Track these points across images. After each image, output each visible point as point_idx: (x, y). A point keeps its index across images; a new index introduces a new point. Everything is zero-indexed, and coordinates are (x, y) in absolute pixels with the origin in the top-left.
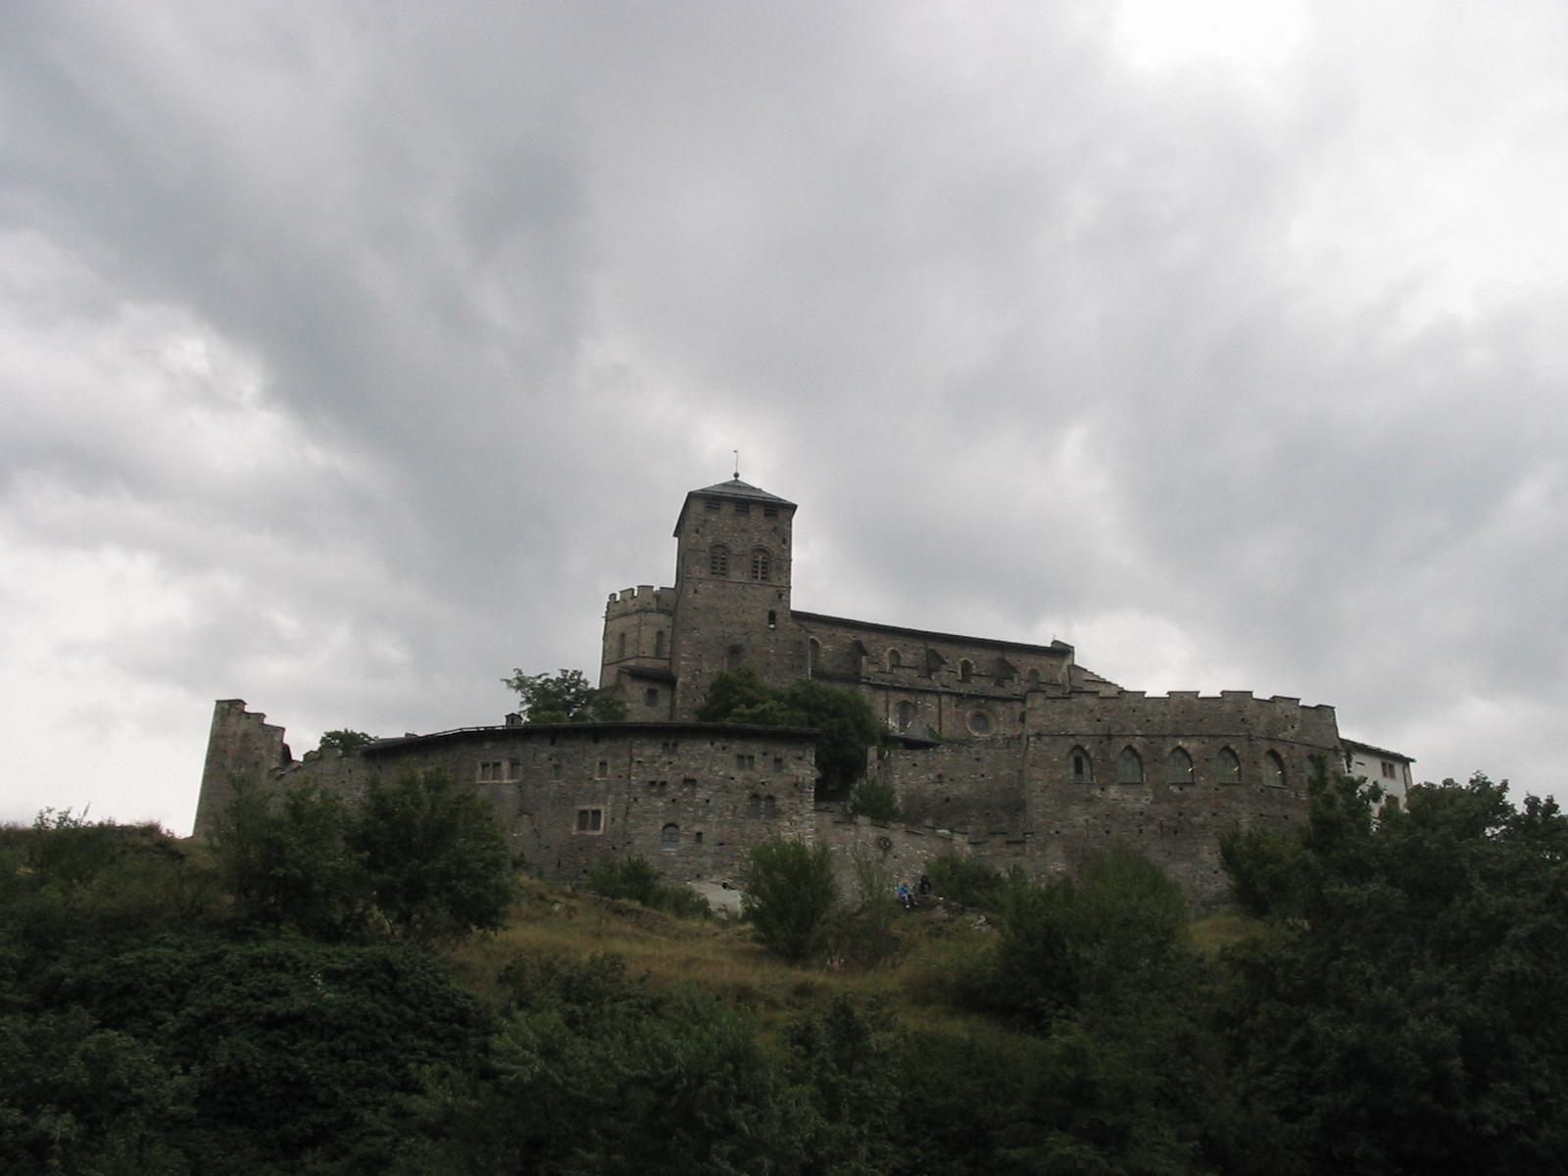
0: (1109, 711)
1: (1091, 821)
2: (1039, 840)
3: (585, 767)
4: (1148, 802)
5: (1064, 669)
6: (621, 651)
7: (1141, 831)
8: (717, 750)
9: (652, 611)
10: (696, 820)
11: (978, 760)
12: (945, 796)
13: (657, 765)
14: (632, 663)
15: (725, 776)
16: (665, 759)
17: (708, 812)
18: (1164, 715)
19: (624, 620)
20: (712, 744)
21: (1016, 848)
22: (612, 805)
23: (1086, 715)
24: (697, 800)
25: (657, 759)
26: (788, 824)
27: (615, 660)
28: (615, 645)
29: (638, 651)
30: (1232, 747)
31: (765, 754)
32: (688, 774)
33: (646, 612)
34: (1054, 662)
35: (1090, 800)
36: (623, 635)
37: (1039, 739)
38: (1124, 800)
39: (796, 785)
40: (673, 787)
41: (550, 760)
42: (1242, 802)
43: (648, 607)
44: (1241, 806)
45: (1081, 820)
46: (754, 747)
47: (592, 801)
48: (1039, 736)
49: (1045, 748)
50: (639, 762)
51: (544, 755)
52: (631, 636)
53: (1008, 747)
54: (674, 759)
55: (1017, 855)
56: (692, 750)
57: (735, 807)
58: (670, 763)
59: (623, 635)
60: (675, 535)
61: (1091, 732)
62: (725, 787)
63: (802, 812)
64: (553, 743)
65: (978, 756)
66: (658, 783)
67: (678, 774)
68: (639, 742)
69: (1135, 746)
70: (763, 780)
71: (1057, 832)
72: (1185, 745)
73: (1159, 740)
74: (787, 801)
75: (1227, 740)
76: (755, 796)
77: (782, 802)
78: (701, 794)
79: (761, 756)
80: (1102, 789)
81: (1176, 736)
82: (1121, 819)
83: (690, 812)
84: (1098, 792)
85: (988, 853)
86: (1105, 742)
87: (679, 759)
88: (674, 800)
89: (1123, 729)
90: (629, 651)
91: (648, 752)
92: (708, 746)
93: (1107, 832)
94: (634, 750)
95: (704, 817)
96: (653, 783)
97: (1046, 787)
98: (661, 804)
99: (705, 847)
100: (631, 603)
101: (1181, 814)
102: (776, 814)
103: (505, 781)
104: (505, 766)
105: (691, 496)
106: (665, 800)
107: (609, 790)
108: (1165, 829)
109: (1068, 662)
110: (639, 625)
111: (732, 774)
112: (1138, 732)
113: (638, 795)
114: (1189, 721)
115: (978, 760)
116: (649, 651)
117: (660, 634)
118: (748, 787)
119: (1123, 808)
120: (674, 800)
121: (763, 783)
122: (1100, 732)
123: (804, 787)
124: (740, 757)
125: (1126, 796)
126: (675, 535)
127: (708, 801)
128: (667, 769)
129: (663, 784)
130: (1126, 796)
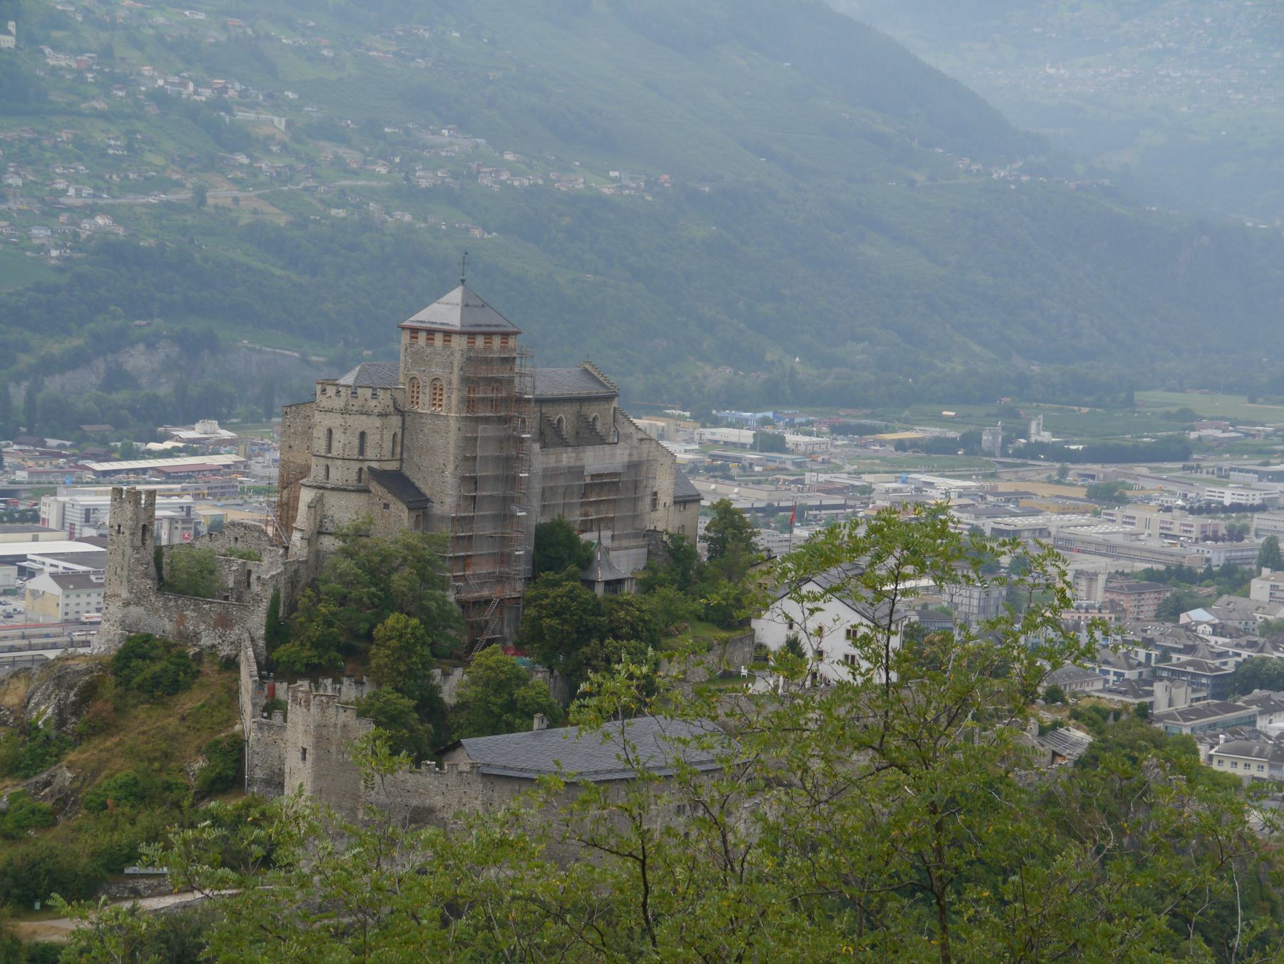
5: (612, 410)
6: (362, 450)
14: (375, 465)
19: (364, 418)
27: (356, 457)
28: (356, 442)
33: (386, 415)
34: (606, 406)
36: (363, 435)
52: (372, 439)
59: (363, 435)
90: (370, 453)
96: (679, 806)
100: (374, 403)
107: (657, 816)
109: (615, 404)
116: (388, 456)
117: (395, 435)
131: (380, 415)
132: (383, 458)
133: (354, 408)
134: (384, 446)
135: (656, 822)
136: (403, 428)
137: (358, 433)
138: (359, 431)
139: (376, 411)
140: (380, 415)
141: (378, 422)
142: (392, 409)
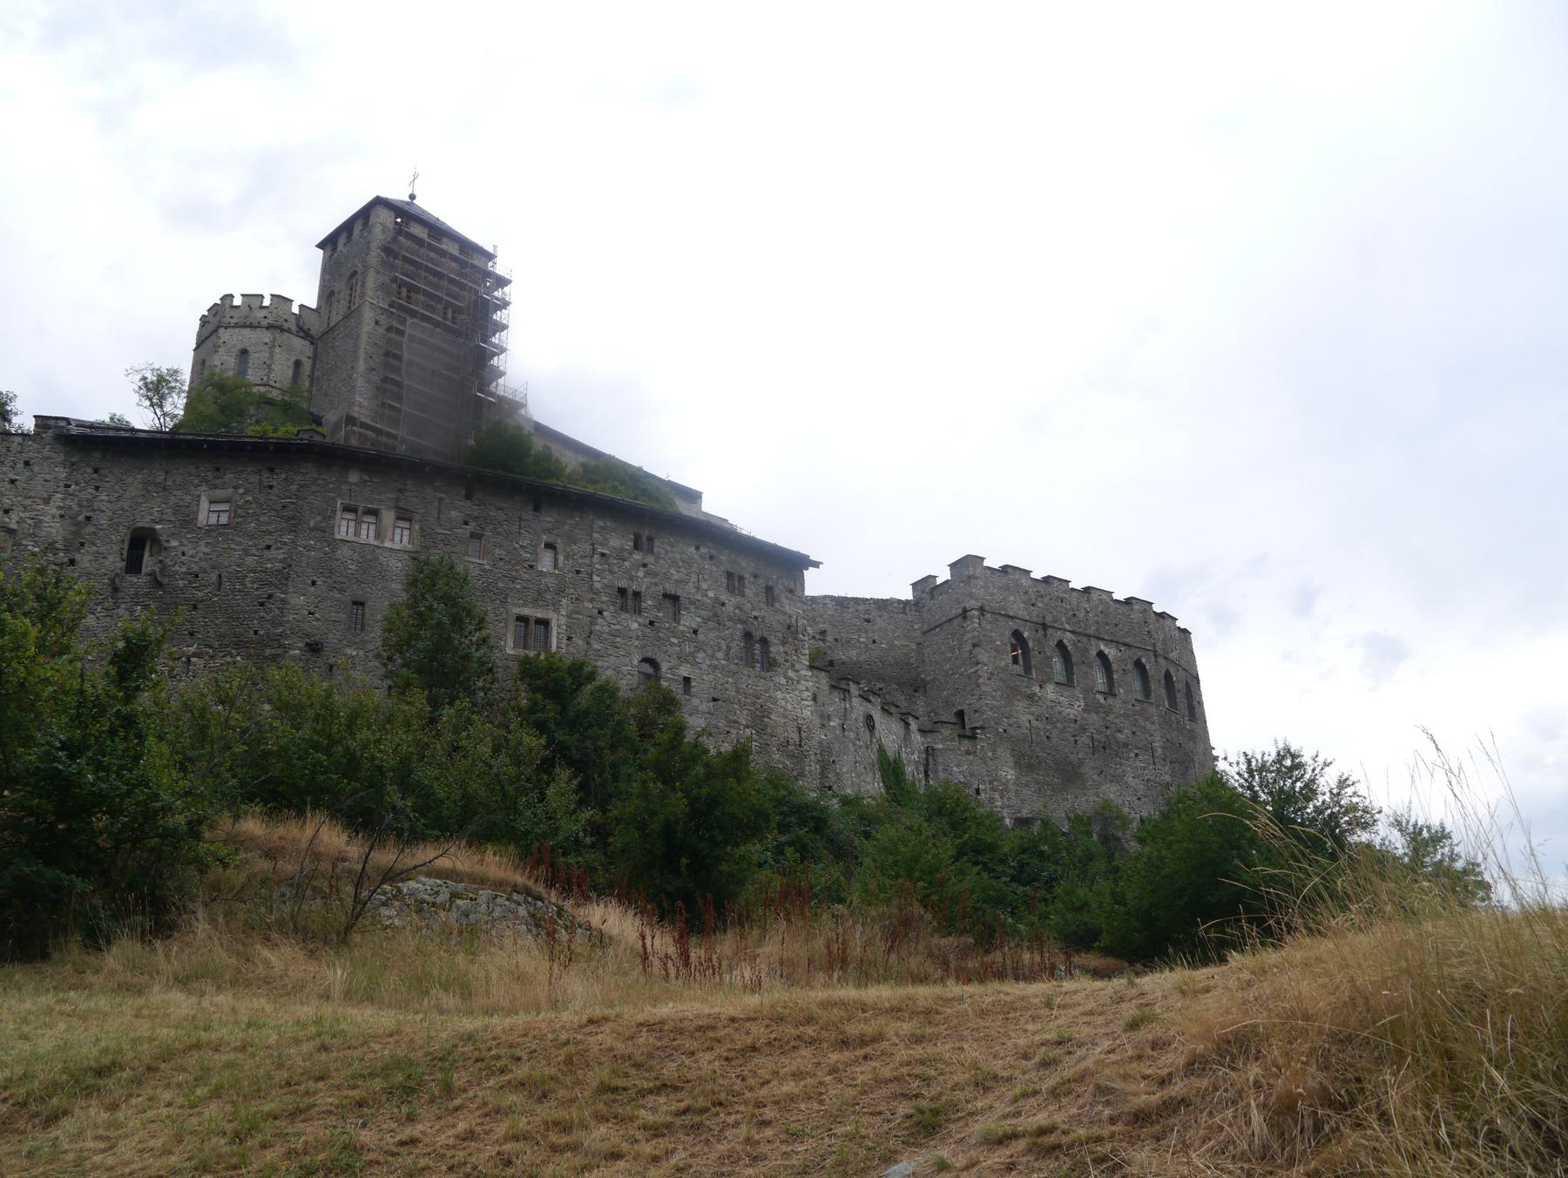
0: (1042, 597)
1: (1035, 723)
2: (989, 738)
3: (522, 547)
4: (1080, 709)
7: (1076, 741)
8: (702, 557)
9: (289, 331)
10: (682, 658)
11: (868, 621)
12: (829, 658)
13: (627, 564)
15: (716, 599)
16: (637, 556)
17: (698, 648)
18: (1087, 612)
19: (246, 332)
20: (697, 548)
21: (966, 744)
22: (568, 617)
23: (1022, 597)
24: (681, 628)
25: (626, 554)
26: (783, 681)
29: (269, 378)
30: (1144, 661)
31: (755, 576)
32: (670, 588)
33: (282, 330)
35: (1031, 697)
37: (983, 615)
38: (1059, 703)
39: (789, 627)
40: (650, 602)
41: (466, 523)
42: (1153, 723)
43: (286, 326)
44: (1154, 728)
45: (1025, 718)
46: (744, 564)
47: (538, 598)
48: (982, 610)
49: (988, 627)
50: (603, 555)
51: (454, 514)
52: (255, 358)
53: (904, 613)
54: (650, 559)
55: (968, 753)
56: (672, 552)
57: (729, 648)
58: (645, 565)
59: (244, 352)
60: (321, 245)
61: (1027, 618)
62: (715, 615)
63: (798, 666)
64: (468, 497)
65: (867, 616)
66: (630, 592)
67: (656, 584)
68: (601, 523)
69: (1065, 641)
70: (755, 613)
71: (1005, 731)
72: (1106, 651)
73: (1085, 640)
74: (781, 649)
75: (1140, 654)
76: (748, 636)
77: (776, 650)
78: (688, 620)
79: (752, 579)
80: (1041, 687)
81: (1099, 639)
82: (1059, 725)
83: (672, 644)
84: (1037, 689)
85: (940, 746)
86: (1041, 632)
87: (657, 560)
88: (651, 623)
89: (1055, 622)
91: (615, 542)
92: (692, 550)
93: (1048, 738)
94: (596, 535)
95: (692, 654)
96: (622, 591)
97: (992, 674)
98: (635, 626)
99: (695, 702)
101: (1107, 728)
102: (770, 664)
103: (388, 544)
104: (388, 517)
105: (378, 202)
106: (641, 620)
107: (560, 591)
108: (1096, 744)
110: (272, 346)
111: (723, 598)
112: (1067, 627)
113: (604, 606)
114: (1107, 624)
115: (868, 621)
117: (298, 364)
118: (740, 621)
119: (1060, 713)
120: (651, 623)
121: (756, 618)
122: (1035, 620)
123: (797, 632)
124: (730, 575)
125: (1062, 699)
126: (321, 245)
127: (695, 632)
128: (641, 574)
129: (637, 595)
130: (1062, 699)
131: (269, 327)
132: (272, 383)
133: (233, 321)
134: (275, 367)
135: (556, 606)
136: (315, 358)
137: (235, 351)
138: (239, 347)
139: (264, 323)
140: (269, 327)
141: (267, 336)
142: (294, 328)
